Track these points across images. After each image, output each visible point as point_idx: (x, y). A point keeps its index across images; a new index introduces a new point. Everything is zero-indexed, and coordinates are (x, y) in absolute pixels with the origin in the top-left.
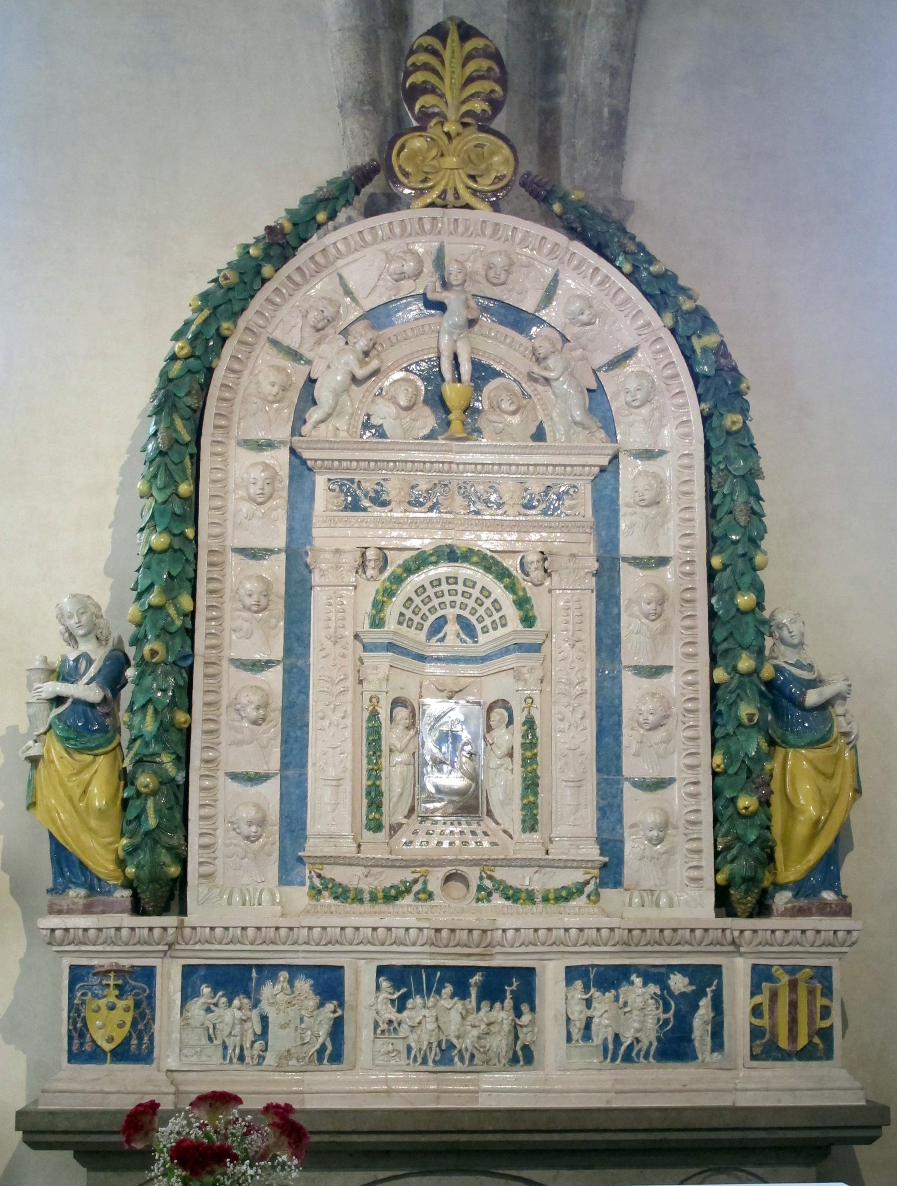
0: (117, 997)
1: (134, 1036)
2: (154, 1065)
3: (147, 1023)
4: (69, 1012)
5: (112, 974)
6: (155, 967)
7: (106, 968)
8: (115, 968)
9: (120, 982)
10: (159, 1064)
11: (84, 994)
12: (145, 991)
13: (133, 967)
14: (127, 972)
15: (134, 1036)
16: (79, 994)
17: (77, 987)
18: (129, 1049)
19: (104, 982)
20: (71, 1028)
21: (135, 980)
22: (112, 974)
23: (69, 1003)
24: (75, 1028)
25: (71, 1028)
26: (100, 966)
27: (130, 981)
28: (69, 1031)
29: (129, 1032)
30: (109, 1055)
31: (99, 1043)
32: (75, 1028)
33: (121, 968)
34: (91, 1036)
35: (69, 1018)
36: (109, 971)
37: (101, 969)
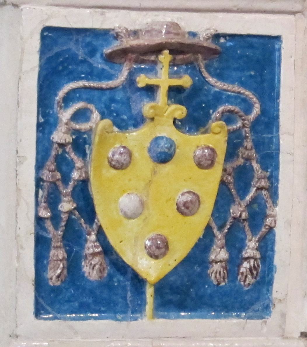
0: (178, 124)
1: (219, 236)
2: (273, 319)
3: (254, 200)
4: (40, 166)
5: (165, 57)
6: (278, 38)
7: (144, 41)
8: (175, 39)
9: (186, 81)
10: (283, 316)
11: (79, 116)
12: (248, 110)
13: (217, 36)
14: (209, 52)
15: (219, 236)
16: (66, 115)
17: (61, 94)
18: (204, 276)
19: (142, 80)
20: (45, 213)
21: (220, 77)
22: (165, 57)
23: (39, 141)
24: (55, 218)
25: (45, 213)
26: (135, 33)
27: (211, 80)
28: (39, 220)
29: (208, 228)
30: (150, 291)
31: (128, 258)
32: (55, 218)
33: (188, 40)
34: (101, 233)
35: (39, 182)
36: (157, 49)
37: (133, 42)
